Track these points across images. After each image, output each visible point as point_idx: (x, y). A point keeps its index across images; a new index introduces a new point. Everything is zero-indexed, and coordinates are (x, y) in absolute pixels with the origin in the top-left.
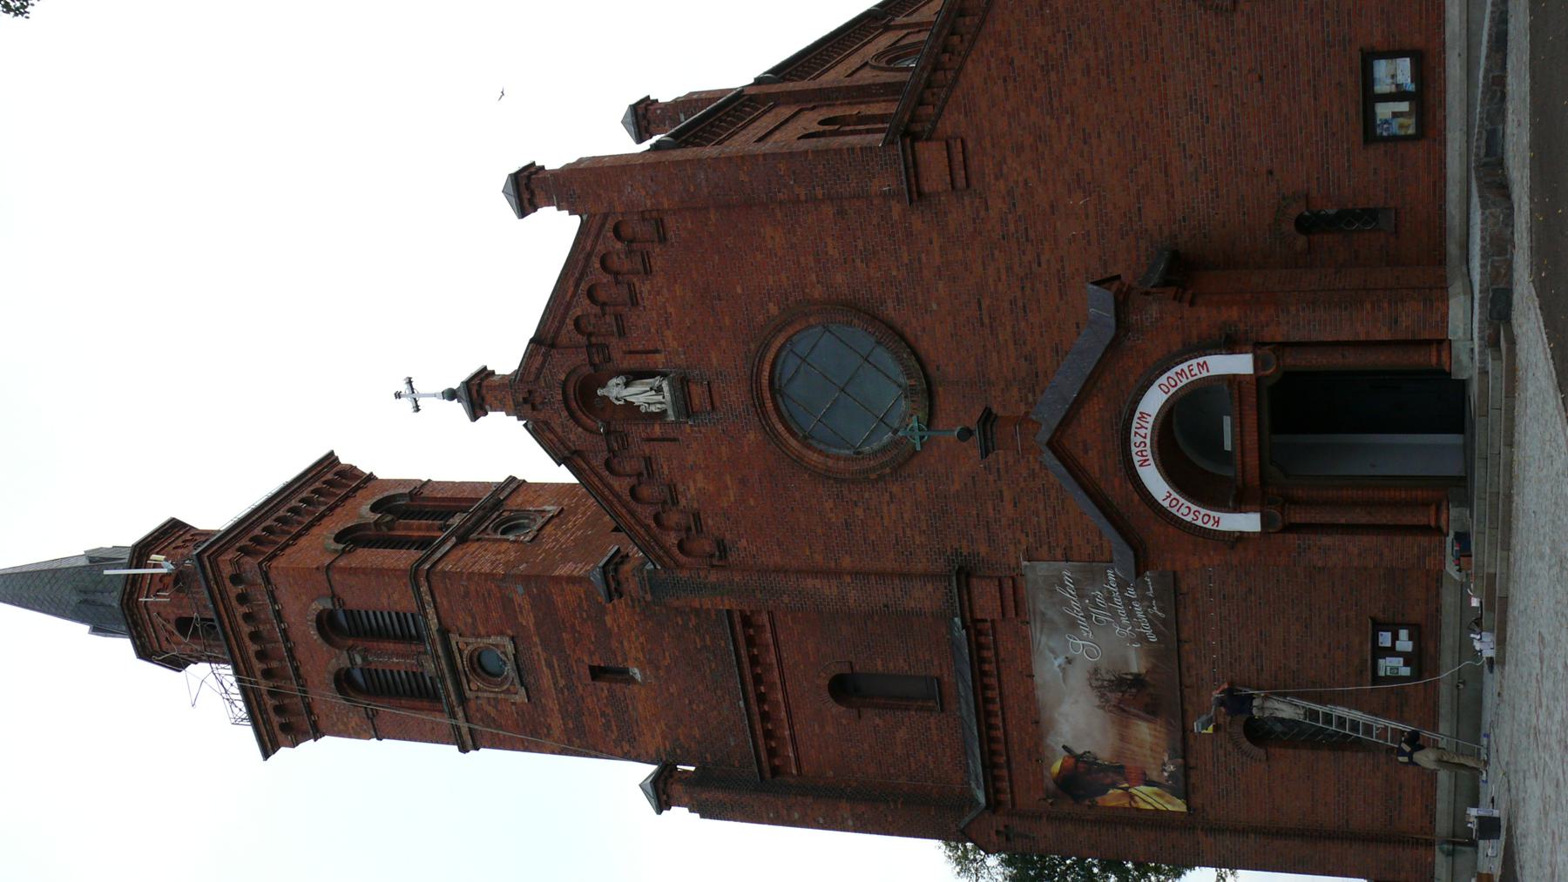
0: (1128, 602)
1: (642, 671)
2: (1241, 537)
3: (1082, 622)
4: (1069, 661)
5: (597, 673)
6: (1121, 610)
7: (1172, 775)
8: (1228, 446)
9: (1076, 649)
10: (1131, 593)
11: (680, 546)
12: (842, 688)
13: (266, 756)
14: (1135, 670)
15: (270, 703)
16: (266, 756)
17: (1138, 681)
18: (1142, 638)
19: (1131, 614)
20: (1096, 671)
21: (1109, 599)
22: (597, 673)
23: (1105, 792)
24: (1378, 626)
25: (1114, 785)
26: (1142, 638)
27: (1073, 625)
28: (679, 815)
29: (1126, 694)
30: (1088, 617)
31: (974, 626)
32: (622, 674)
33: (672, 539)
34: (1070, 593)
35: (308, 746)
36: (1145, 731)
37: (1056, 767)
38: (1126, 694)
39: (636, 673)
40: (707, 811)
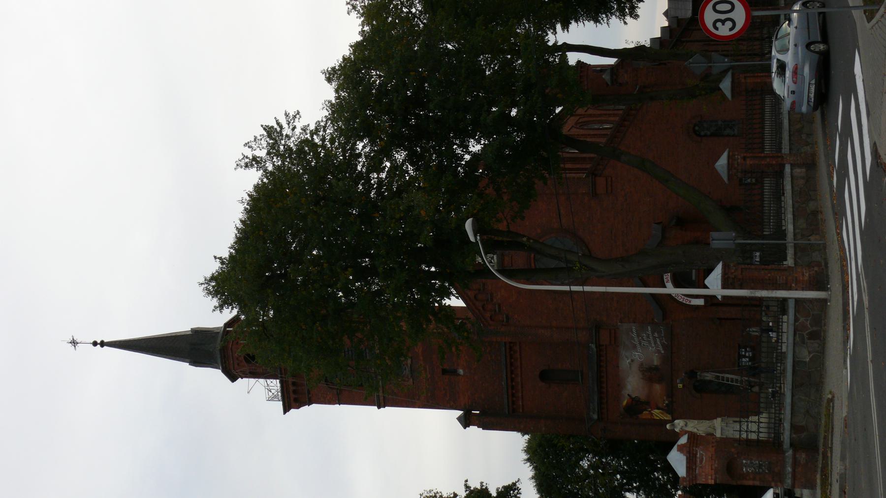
0: (654, 338)
1: (464, 370)
2: (697, 307)
3: (638, 346)
4: (632, 361)
5: (444, 372)
6: (652, 342)
7: (667, 405)
8: (694, 278)
9: (635, 355)
10: (656, 335)
11: (491, 318)
12: (544, 376)
13: (285, 412)
14: (656, 363)
15: (292, 388)
16: (285, 412)
17: (656, 368)
18: (659, 352)
19: (655, 343)
20: (642, 364)
21: (648, 337)
22: (444, 372)
23: (641, 412)
24: (740, 347)
25: (646, 410)
26: (659, 352)
27: (635, 347)
28: (473, 429)
29: (650, 374)
30: (640, 344)
31: (599, 346)
32: (454, 372)
33: (488, 315)
34: (634, 335)
35: (305, 409)
36: (658, 388)
37: (625, 403)
38: (650, 374)
39: (461, 372)
40: (486, 427)
